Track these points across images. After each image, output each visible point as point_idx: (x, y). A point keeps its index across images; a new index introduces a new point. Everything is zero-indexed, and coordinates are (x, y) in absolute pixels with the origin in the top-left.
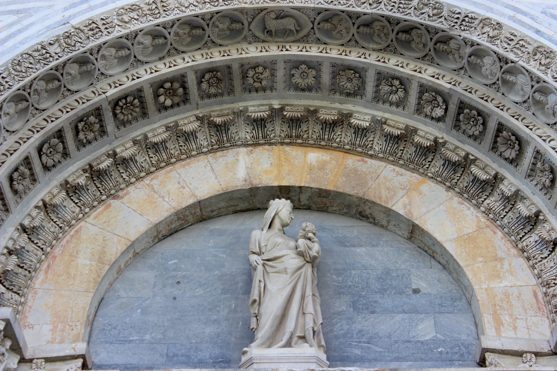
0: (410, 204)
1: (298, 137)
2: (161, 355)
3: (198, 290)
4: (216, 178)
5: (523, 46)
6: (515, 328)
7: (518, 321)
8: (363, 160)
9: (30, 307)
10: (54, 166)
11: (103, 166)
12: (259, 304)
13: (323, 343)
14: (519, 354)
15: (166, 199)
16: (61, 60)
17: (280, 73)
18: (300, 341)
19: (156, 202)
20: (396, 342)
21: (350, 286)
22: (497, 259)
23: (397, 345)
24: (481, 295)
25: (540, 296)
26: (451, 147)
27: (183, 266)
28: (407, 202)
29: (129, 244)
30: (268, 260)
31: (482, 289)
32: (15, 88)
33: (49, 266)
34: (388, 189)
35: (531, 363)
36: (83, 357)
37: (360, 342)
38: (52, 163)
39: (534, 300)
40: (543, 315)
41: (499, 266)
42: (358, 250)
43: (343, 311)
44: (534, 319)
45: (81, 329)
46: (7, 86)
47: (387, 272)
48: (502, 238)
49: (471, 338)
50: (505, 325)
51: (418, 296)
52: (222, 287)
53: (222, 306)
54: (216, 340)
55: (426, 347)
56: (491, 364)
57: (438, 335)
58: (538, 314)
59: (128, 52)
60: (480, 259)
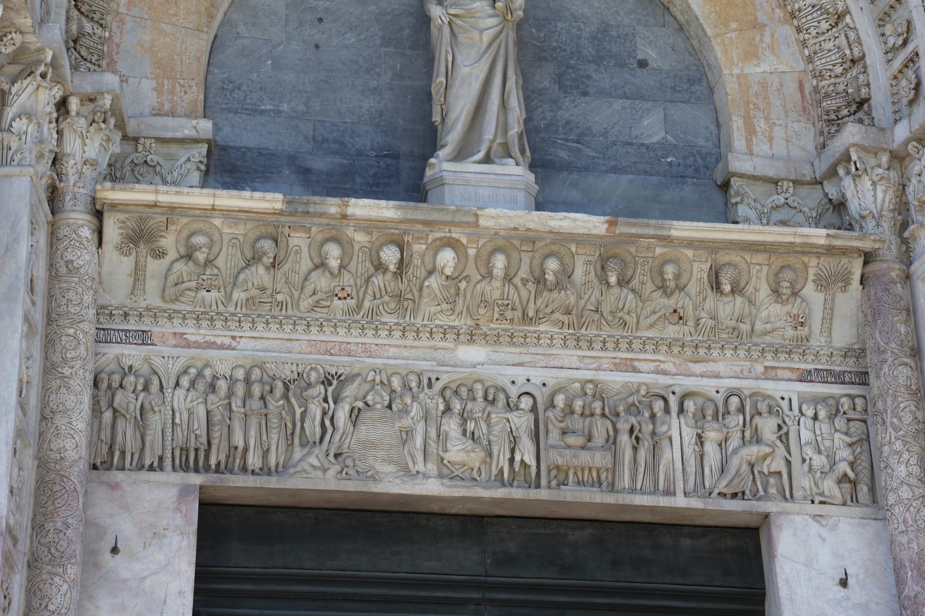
2: (306, 138)
3: (348, 36)
6: (771, 139)
7: (776, 128)
9: (118, 46)
14: (775, 182)
20: (614, 143)
21: (555, 49)
22: (757, 26)
23: (614, 148)
24: (730, 87)
25: (808, 89)
30: (455, 16)
31: (733, 75)
35: (787, 195)
36: (209, 142)
37: (567, 140)
39: (799, 95)
40: (809, 120)
41: (757, 38)
43: (545, 89)
44: (796, 126)
45: (196, 94)
47: (605, 28)
49: (710, 144)
51: (644, 71)
52: (381, 33)
53: (383, 66)
54: (377, 120)
55: (652, 155)
56: (737, 194)
57: (669, 137)
58: (802, 118)
60: (734, 25)
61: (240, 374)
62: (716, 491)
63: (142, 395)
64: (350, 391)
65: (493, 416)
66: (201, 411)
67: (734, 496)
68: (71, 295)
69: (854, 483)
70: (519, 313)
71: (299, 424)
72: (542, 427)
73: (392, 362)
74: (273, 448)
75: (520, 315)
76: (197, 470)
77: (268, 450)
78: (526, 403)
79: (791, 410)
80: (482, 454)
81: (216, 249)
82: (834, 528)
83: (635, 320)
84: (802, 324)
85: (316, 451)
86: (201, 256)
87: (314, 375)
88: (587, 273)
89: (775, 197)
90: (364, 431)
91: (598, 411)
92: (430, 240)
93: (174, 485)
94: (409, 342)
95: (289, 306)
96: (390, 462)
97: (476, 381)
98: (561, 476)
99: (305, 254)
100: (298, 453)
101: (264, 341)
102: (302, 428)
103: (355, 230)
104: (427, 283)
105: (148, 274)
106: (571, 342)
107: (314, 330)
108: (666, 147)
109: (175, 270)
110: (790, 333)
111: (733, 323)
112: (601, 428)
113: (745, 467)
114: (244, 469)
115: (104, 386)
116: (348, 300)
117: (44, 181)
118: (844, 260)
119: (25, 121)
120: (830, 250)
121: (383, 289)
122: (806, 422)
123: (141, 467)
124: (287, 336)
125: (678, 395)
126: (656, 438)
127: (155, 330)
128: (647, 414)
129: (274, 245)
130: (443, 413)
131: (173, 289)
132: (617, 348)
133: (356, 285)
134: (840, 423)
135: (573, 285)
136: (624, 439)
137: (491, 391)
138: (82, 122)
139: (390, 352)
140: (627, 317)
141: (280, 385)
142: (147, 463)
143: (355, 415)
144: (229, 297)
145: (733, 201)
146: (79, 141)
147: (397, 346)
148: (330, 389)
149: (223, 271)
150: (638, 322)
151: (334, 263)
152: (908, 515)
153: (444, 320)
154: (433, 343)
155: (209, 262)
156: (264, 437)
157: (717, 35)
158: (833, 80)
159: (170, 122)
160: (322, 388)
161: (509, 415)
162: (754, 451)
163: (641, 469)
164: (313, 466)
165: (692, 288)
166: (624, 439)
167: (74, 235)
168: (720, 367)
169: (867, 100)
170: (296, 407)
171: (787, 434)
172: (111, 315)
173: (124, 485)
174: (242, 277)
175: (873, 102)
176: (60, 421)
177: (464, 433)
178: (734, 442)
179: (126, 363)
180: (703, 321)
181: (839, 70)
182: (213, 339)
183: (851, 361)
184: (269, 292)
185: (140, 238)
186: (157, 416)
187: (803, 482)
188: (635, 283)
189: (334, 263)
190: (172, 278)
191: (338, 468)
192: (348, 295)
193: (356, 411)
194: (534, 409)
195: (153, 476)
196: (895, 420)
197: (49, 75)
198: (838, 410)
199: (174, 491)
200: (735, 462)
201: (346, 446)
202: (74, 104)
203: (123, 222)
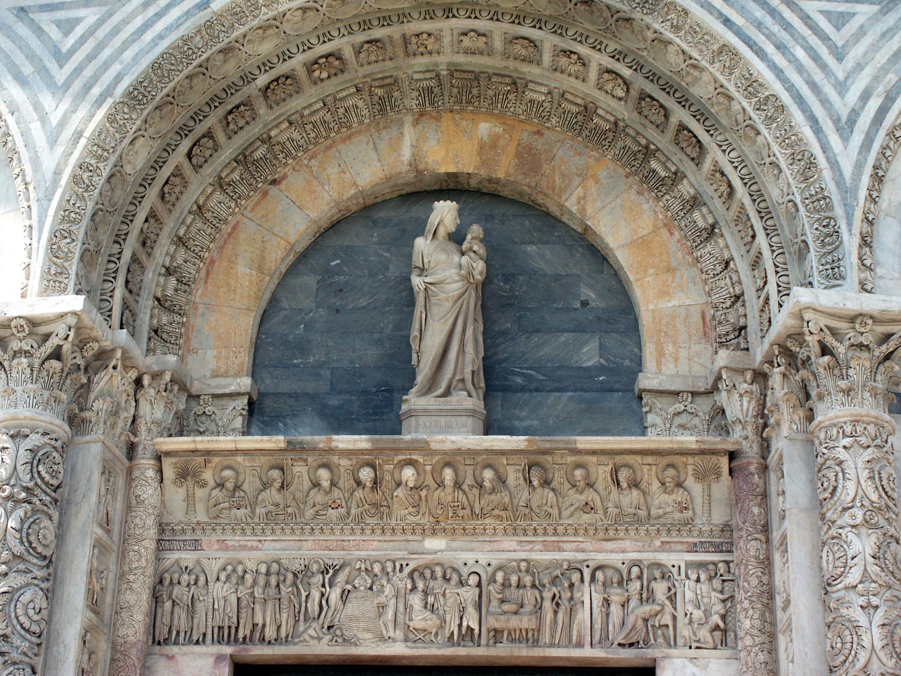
0: (584, 198)
1: (469, 102)
3: (361, 300)
4: (379, 160)
5: (708, 41)
6: (676, 360)
8: (539, 133)
9: (193, 326)
10: (205, 161)
11: (258, 154)
12: (420, 339)
13: (483, 385)
14: (677, 394)
15: (326, 188)
16: (205, 56)
17: (447, 40)
18: (460, 385)
19: (315, 191)
22: (670, 270)
26: (631, 132)
27: (346, 269)
28: (581, 194)
29: (288, 248)
31: (648, 310)
32: (158, 98)
33: (208, 274)
34: (563, 175)
36: (249, 394)
38: (204, 159)
40: (708, 341)
41: (670, 280)
42: (531, 249)
45: (245, 358)
46: (150, 97)
48: (678, 241)
50: (667, 356)
56: (646, 405)
57: (602, 360)
59: (276, 30)
60: (652, 271)
62: (616, 643)
63: (193, 588)
64: (341, 578)
65: (447, 591)
66: (233, 599)
67: (631, 645)
68: (137, 521)
69: (725, 631)
70: (468, 511)
71: (304, 604)
72: (484, 598)
73: (374, 553)
74: (284, 623)
75: (469, 514)
76: (229, 642)
78: (473, 580)
79: (680, 575)
80: (438, 622)
81: (241, 478)
82: (705, 667)
83: (557, 512)
84: (686, 508)
85: (314, 625)
86: (230, 485)
87: (315, 567)
88: (517, 479)
89: (677, 405)
90: (352, 608)
91: (528, 584)
93: (212, 655)
94: (387, 538)
95: (298, 516)
96: (368, 631)
97: (437, 564)
98: (497, 634)
99: (306, 478)
100: (301, 627)
104: (395, 494)
105: (196, 499)
106: (510, 530)
107: (317, 532)
108: (600, 369)
109: (213, 495)
110: (678, 515)
111: (632, 511)
112: (530, 596)
113: (640, 622)
114: (262, 640)
115: (167, 582)
116: (340, 509)
117: (123, 438)
118: (714, 458)
119: (101, 401)
120: (702, 452)
122: (692, 584)
123: (190, 642)
125: (591, 568)
126: (572, 603)
128: (566, 585)
129: (281, 473)
130: (411, 591)
132: (545, 533)
134: (717, 583)
135: (507, 488)
136: (548, 605)
137: (449, 571)
138: (152, 392)
139: (371, 547)
140: (550, 510)
141: (290, 576)
142: (195, 638)
143: (345, 595)
145: (645, 409)
146: (149, 407)
148: (327, 577)
149: (248, 492)
150: (560, 513)
152: (749, 659)
153: (411, 519)
155: (237, 487)
156: (278, 616)
157: (638, 280)
158: (725, 311)
159: (222, 381)
160: (321, 576)
161: (458, 591)
162: (647, 609)
163: (559, 628)
164: (311, 636)
165: (600, 485)
166: (548, 605)
168: (627, 544)
169: (745, 327)
170: (302, 591)
171: (675, 594)
173: (177, 656)
174: (260, 497)
175: (748, 329)
176: (124, 614)
177: (425, 607)
178: (633, 603)
179: (184, 564)
180: (609, 510)
181: (729, 303)
182: (245, 543)
183: (728, 534)
184: (282, 506)
185: (188, 475)
187: (684, 631)
188: (553, 485)
189: (326, 484)
191: (329, 637)
193: (346, 592)
194: (479, 585)
195: (197, 649)
196: (746, 584)
197: (119, 367)
198: (716, 574)
199: (211, 660)
200: (630, 620)
201: (337, 620)
202: (146, 380)
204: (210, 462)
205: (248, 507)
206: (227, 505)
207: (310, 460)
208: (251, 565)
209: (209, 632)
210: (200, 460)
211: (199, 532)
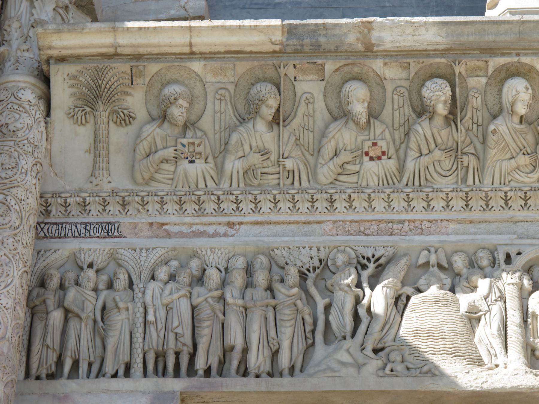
61: (240, 262)
63: (104, 294)
66: (185, 307)
73: (452, 238)
76: (177, 373)
77: (277, 351)
81: (198, 107)
85: (348, 343)
92: (491, 70)
93: (144, 393)
94: (475, 215)
99: (320, 104)
100: (320, 350)
101: (272, 227)
102: (327, 323)
103: (385, 64)
104: (492, 127)
105: (112, 148)
109: (145, 135)
115: (54, 283)
121: (431, 141)
124: (303, 218)
127: (124, 221)
131: (145, 161)
133: (394, 141)
144: (220, 170)
147: (460, 222)
148: (365, 274)
149: (211, 136)
151: (359, 109)
154: (511, 213)
156: (272, 333)
164: (344, 364)
167: (13, 99)
172: (66, 205)
174: (235, 137)
182: (202, 228)
184: (273, 157)
185: (98, 96)
186: (123, 315)
189: (359, 109)
190: (143, 147)
191: (379, 363)
192: (383, 153)
195: (116, 384)
203: (75, 77)
204: (141, 75)
205: (210, 159)
206: (170, 152)
207: (330, 67)
208: (215, 259)
209: (139, 359)
210: (124, 67)
211: (114, 208)
